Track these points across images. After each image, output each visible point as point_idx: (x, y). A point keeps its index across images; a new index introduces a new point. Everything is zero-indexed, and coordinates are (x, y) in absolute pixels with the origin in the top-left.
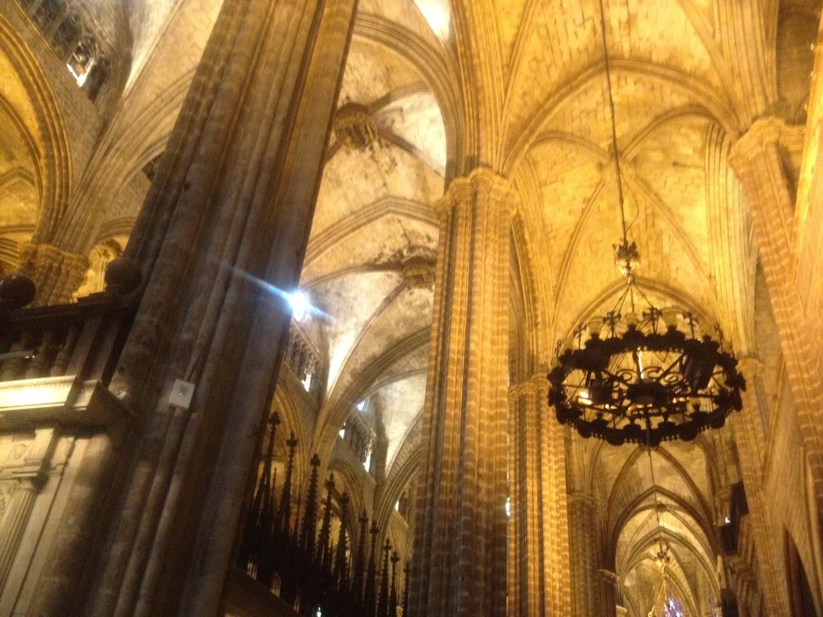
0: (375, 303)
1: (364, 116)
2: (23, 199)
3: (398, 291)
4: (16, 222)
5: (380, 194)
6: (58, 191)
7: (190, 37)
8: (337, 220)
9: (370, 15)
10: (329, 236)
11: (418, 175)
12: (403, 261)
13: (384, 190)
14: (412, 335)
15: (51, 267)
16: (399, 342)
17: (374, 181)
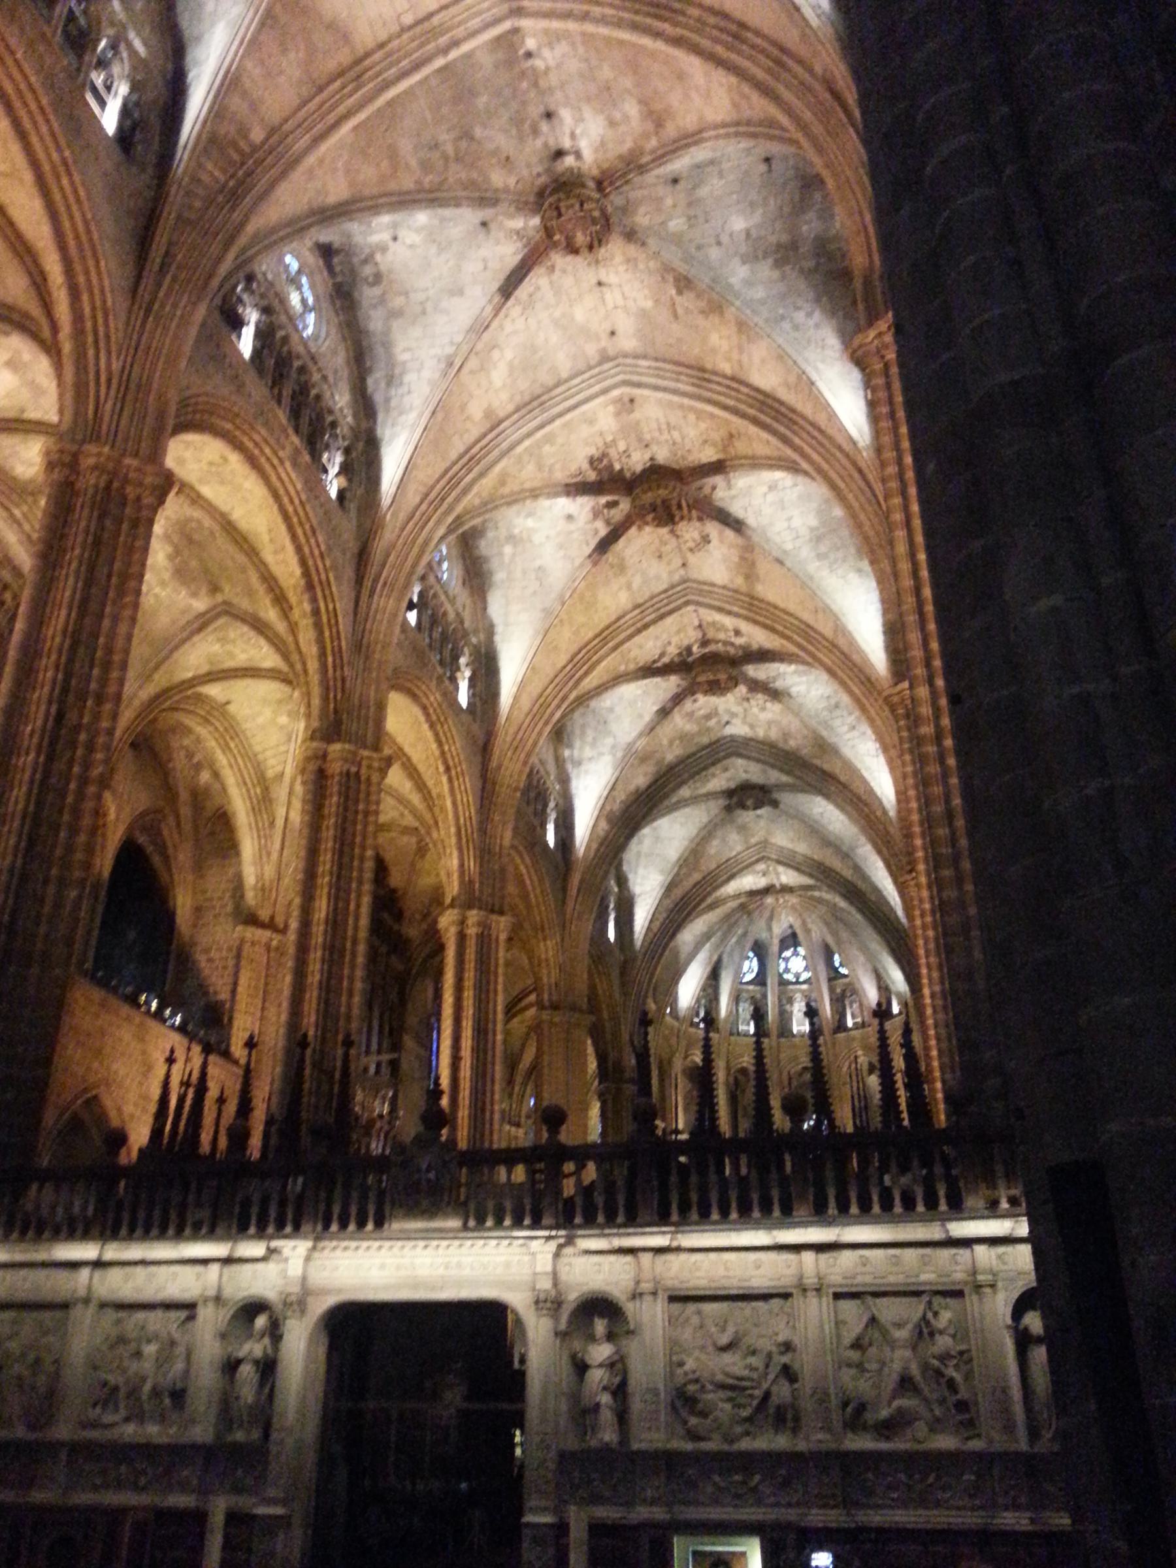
0: (640, 716)
1: (678, 485)
2: (219, 640)
3: (677, 699)
4: (205, 669)
5: (676, 578)
6: (330, 659)
7: (463, 407)
8: (613, 618)
9: (725, 376)
10: (605, 642)
11: (742, 558)
12: (690, 659)
13: (682, 572)
14: (689, 757)
15: (348, 774)
16: (671, 768)
17: (669, 564)
